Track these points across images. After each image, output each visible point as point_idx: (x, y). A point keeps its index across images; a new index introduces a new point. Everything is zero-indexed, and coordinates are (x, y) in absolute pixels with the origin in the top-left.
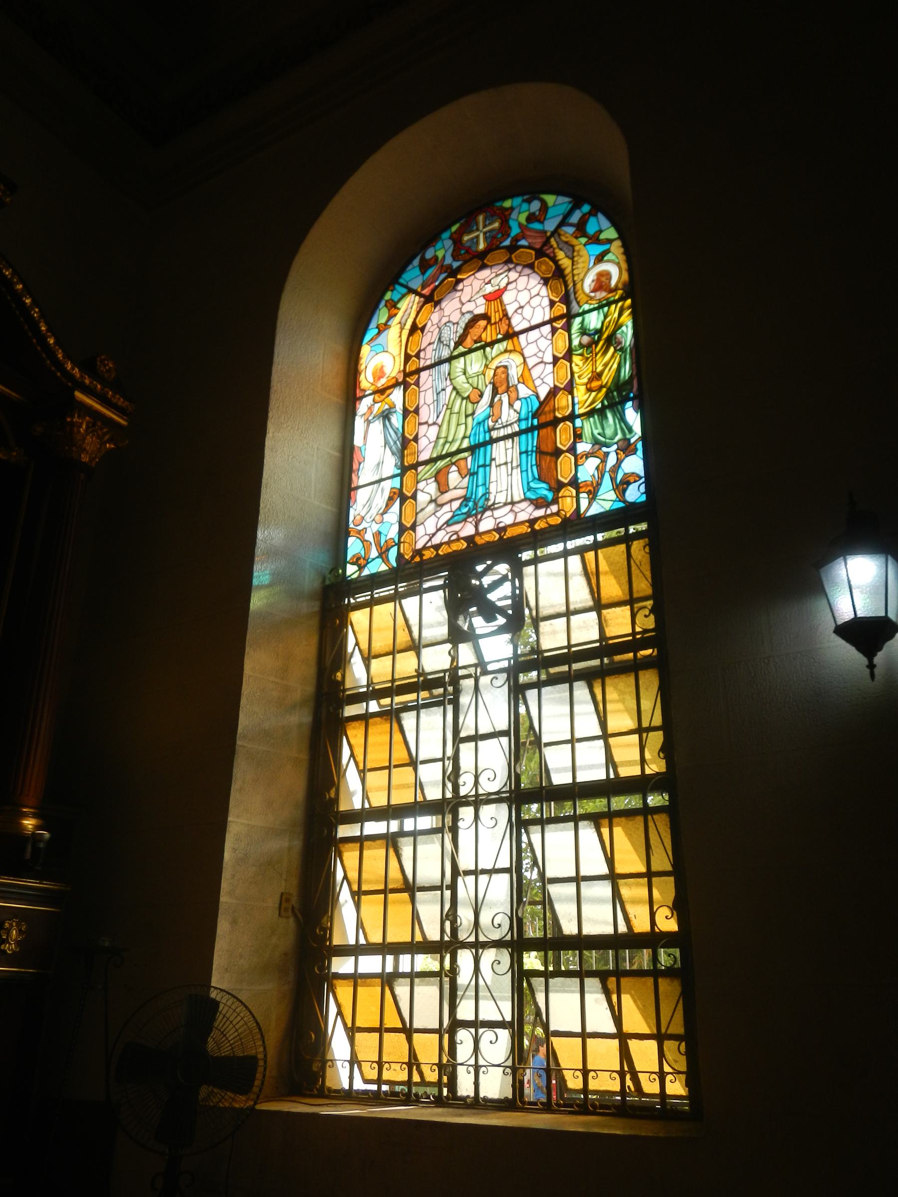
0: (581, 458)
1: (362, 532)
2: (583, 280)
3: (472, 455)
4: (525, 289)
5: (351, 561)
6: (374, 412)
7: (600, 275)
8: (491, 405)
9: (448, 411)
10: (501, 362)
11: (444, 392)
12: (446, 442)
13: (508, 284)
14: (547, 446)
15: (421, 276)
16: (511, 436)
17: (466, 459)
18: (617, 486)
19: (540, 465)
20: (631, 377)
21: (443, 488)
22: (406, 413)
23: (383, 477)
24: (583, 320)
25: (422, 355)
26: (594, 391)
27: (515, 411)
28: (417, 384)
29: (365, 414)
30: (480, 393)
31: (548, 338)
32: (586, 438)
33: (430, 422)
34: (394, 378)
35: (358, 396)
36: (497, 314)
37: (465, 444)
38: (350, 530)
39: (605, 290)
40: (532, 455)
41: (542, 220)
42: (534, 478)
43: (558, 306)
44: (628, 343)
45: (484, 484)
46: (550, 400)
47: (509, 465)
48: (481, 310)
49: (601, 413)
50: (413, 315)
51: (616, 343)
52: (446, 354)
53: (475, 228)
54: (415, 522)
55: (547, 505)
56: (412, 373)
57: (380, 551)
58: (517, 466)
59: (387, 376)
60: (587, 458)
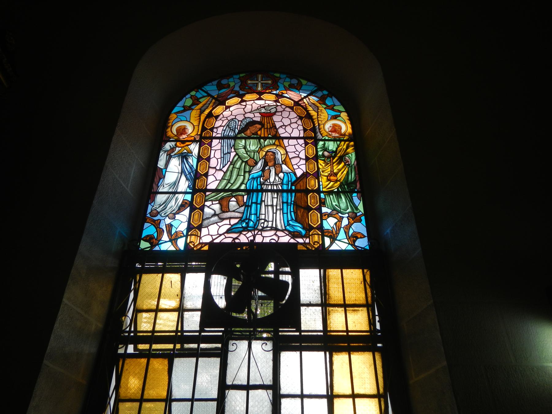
0: (325, 216)
2: (324, 124)
3: (248, 195)
4: (288, 117)
5: (145, 239)
6: (176, 152)
7: (334, 125)
8: (263, 170)
9: (232, 166)
10: (270, 149)
11: (229, 155)
12: (229, 182)
13: (276, 112)
14: (301, 203)
15: (218, 91)
16: (277, 191)
18: (350, 238)
19: (296, 212)
20: (355, 180)
21: (225, 208)
22: (199, 158)
23: (178, 191)
24: (324, 144)
25: (215, 130)
26: (333, 182)
27: (279, 178)
28: (210, 144)
29: (168, 151)
30: (255, 162)
33: (218, 168)
34: (192, 136)
37: (243, 187)
38: (147, 218)
39: (338, 133)
40: (291, 205)
41: (299, 89)
42: (292, 219)
44: (353, 163)
46: (303, 178)
47: (275, 208)
48: (258, 119)
49: (338, 194)
51: (345, 161)
52: (232, 134)
53: (255, 79)
55: (302, 237)
58: (280, 209)
59: (187, 134)
60: (328, 217)
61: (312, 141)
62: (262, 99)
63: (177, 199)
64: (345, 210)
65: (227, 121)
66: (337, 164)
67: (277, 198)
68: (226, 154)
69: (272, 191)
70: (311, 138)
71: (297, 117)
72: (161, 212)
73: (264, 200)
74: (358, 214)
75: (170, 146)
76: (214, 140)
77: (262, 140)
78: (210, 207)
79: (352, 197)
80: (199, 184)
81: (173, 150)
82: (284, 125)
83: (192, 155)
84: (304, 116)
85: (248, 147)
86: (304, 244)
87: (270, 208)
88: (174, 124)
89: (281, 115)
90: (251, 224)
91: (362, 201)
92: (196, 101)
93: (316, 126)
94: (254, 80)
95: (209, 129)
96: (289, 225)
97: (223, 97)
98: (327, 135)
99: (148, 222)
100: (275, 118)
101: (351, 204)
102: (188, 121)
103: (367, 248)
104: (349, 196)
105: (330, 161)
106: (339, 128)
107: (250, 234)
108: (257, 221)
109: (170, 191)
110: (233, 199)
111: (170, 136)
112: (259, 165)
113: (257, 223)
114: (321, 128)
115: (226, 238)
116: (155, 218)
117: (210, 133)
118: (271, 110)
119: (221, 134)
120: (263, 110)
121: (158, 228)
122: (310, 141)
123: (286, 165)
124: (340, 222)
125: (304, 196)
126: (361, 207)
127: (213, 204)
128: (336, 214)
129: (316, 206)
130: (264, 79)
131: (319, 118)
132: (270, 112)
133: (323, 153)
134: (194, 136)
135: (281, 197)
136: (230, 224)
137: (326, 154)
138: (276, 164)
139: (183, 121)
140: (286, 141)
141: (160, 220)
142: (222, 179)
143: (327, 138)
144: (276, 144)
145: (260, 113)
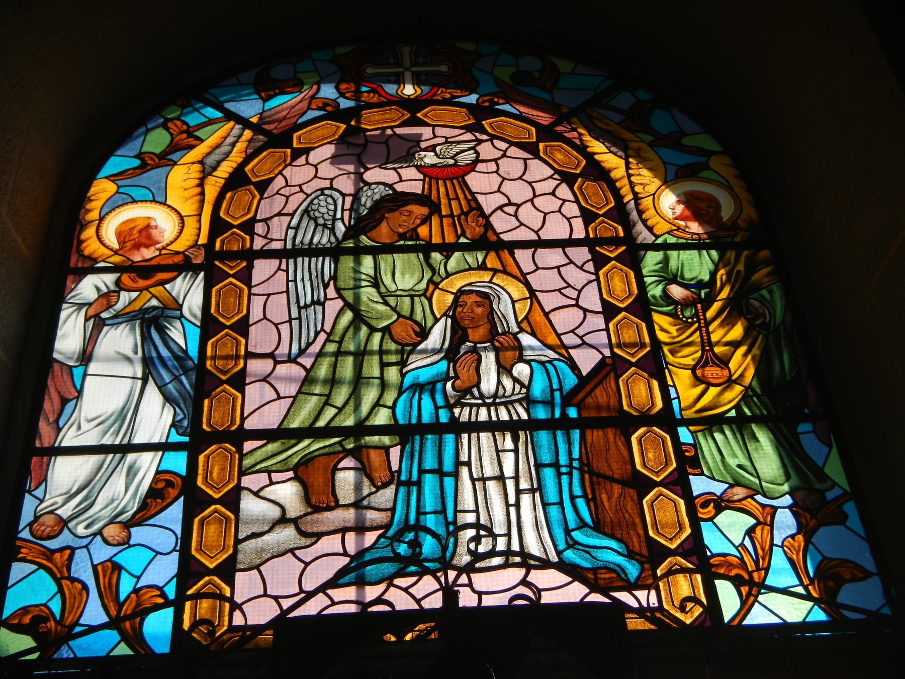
0: (705, 505)
1: (57, 556)
4: (520, 178)
6: (119, 306)
8: (451, 354)
10: (470, 284)
11: (319, 308)
12: (327, 403)
13: (477, 161)
15: (260, 102)
16: (513, 427)
17: (386, 449)
18: (812, 581)
19: (594, 499)
23: (138, 440)
24: (666, 261)
25: (259, 228)
27: (516, 380)
28: (246, 277)
30: (417, 329)
31: (586, 267)
32: (709, 469)
34: (177, 253)
35: (72, 265)
36: (454, 204)
37: (382, 418)
38: (18, 543)
40: (570, 474)
42: (582, 525)
43: (603, 222)
44: (779, 319)
46: (605, 377)
47: (510, 485)
48: (416, 188)
50: (236, 157)
52: (324, 241)
54: (233, 558)
56: (227, 256)
57: (114, 613)
59: (158, 246)
60: (719, 510)
61: (620, 251)
62: (424, 124)
63: (134, 469)
64: (779, 482)
65: (302, 196)
66: (722, 325)
67: (516, 451)
68: (310, 306)
69: (493, 427)
70: (615, 241)
71: (554, 177)
72: (74, 522)
73: (466, 459)
74: (830, 495)
75: (98, 289)
76: (258, 263)
77: (436, 256)
78: (262, 494)
79: (796, 435)
80: (216, 417)
81: (109, 301)
82: (510, 204)
83: (182, 316)
84: (578, 172)
85: (387, 279)
86: (642, 612)
87: (492, 486)
88: (107, 214)
89: (497, 172)
90: (429, 545)
91: (834, 451)
92: (184, 136)
93: (628, 202)
94: (388, 65)
95: (238, 227)
96: (573, 544)
97: (280, 121)
98: (672, 231)
99: (24, 560)
100: (475, 181)
101: (797, 460)
102: (161, 203)
103: (886, 611)
104: (786, 431)
105: (696, 315)
106: (709, 207)
107: (428, 583)
108: (449, 534)
109: (107, 440)
110: (348, 462)
111: (95, 256)
112: (435, 339)
113: (451, 546)
114: (648, 209)
115: (334, 603)
116: (53, 544)
117: (244, 240)
118: (459, 158)
119: (285, 240)
121: (63, 578)
122: (611, 252)
123: (533, 334)
124: (767, 528)
125: (615, 442)
126: (834, 469)
127: (272, 483)
128: (744, 499)
129: (666, 474)
130: (421, 60)
131: (633, 175)
132: (455, 165)
133: (665, 290)
134: (183, 253)
135: (530, 446)
136: (345, 554)
137: (677, 292)
138: (498, 334)
139: (142, 201)
140: (523, 256)
141: (73, 550)
142: (299, 392)
143: (672, 240)
144: (489, 266)
145: (419, 168)
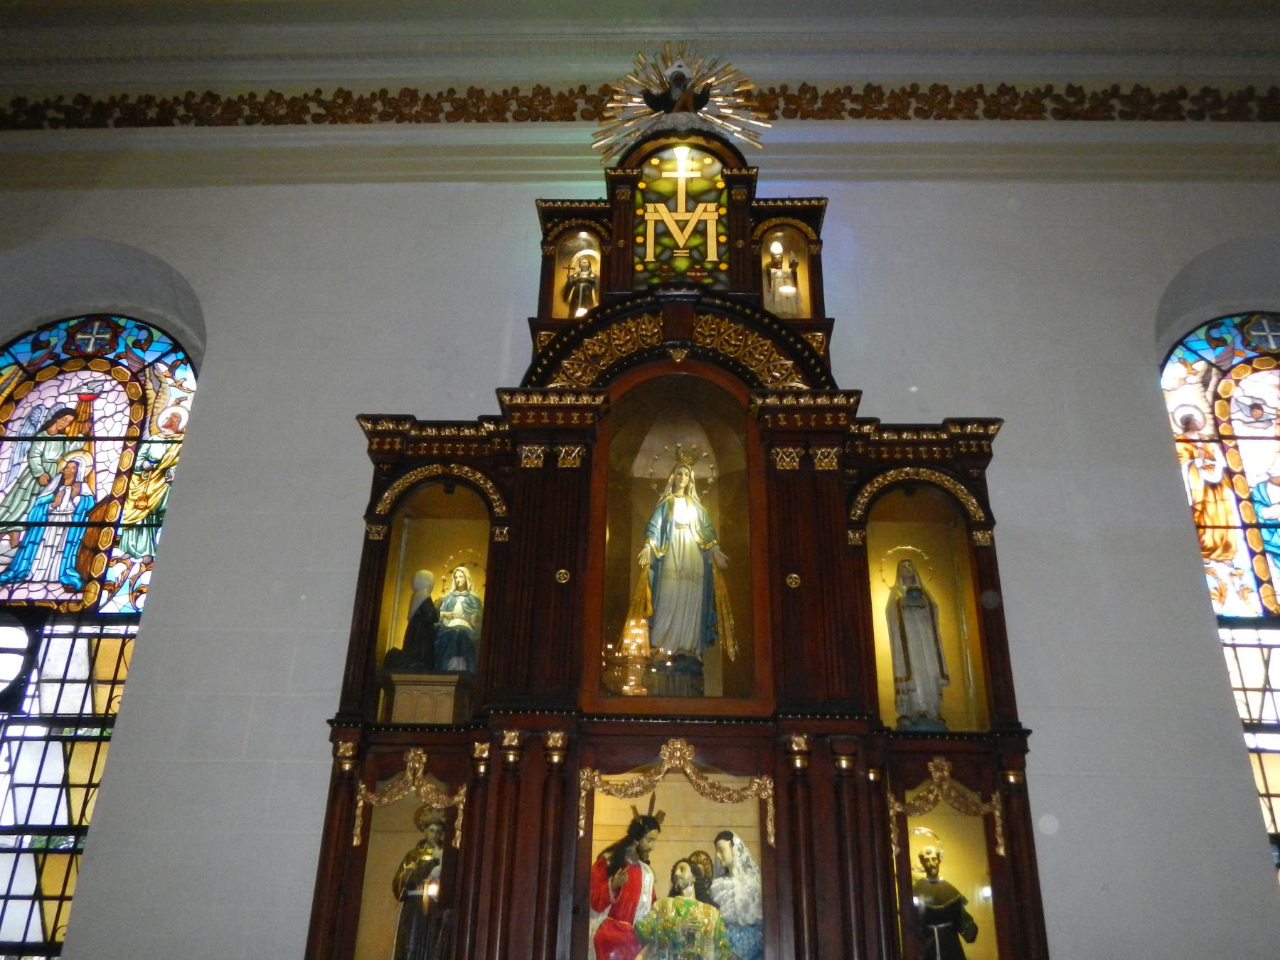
2: (159, 414)
7: (174, 415)
8: (56, 492)
12: (8, 511)
25: (10, 425)
27: (73, 504)
37: (23, 519)
39: (173, 430)
42: (71, 567)
45: (29, 559)
47: (55, 549)
48: (72, 406)
50: (13, 385)
53: (89, 331)
55: (76, 592)
60: (117, 562)
69: (58, 524)
85: (46, 453)
87: (49, 549)
96: (65, 574)
120: (84, 390)
137: (147, 464)
145: (78, 394)
